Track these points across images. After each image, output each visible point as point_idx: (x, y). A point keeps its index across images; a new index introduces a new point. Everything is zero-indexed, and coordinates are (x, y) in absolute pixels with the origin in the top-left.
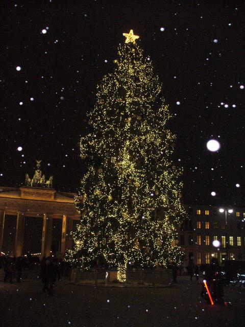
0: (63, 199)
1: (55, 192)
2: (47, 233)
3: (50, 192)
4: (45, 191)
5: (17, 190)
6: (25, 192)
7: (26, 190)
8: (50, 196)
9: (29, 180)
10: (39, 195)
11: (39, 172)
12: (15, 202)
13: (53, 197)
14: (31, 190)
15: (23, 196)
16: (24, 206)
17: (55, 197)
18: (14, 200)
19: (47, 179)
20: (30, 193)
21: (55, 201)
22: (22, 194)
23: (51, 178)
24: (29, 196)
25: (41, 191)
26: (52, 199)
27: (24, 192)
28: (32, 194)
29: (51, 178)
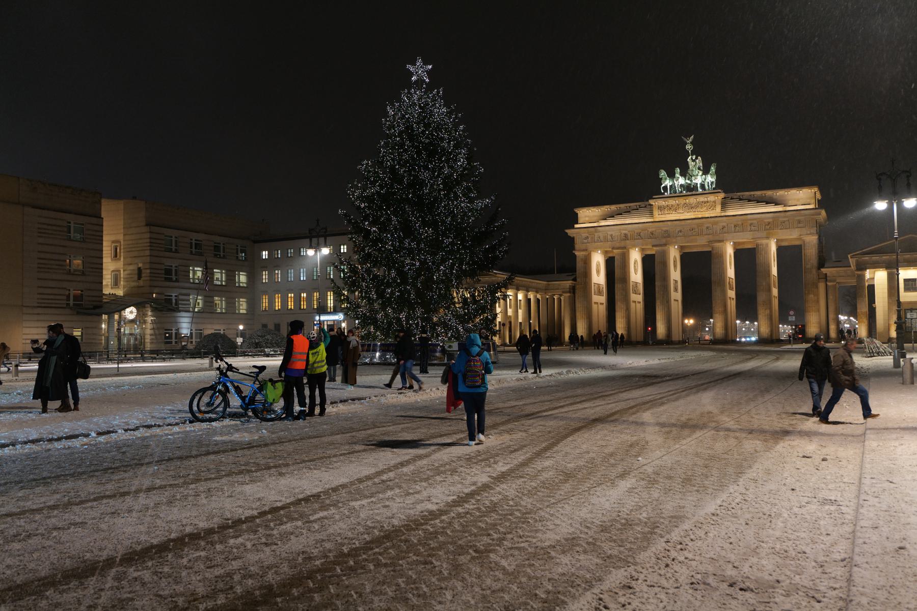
0: (742, 207)
1: (722, 195)
3: (711, 198)
4: (701, 199)
6: (660, 208)
7: (661, 202)
8: (713, 206)
9: (668, 183)
10: (691, 207)
11: (693, 161)
12: (644, 230)
13: (719, 208)
14: (671, 202)
15: (658, 216)
17: (724, 206)
20: (670, 208)
21: (723, 214)
23: (713, 169)
24: (666, 212)
25: (692, 200)
26: (717, 211)
27: (660, 208)
28: (674, 208)
29: (713, 169)
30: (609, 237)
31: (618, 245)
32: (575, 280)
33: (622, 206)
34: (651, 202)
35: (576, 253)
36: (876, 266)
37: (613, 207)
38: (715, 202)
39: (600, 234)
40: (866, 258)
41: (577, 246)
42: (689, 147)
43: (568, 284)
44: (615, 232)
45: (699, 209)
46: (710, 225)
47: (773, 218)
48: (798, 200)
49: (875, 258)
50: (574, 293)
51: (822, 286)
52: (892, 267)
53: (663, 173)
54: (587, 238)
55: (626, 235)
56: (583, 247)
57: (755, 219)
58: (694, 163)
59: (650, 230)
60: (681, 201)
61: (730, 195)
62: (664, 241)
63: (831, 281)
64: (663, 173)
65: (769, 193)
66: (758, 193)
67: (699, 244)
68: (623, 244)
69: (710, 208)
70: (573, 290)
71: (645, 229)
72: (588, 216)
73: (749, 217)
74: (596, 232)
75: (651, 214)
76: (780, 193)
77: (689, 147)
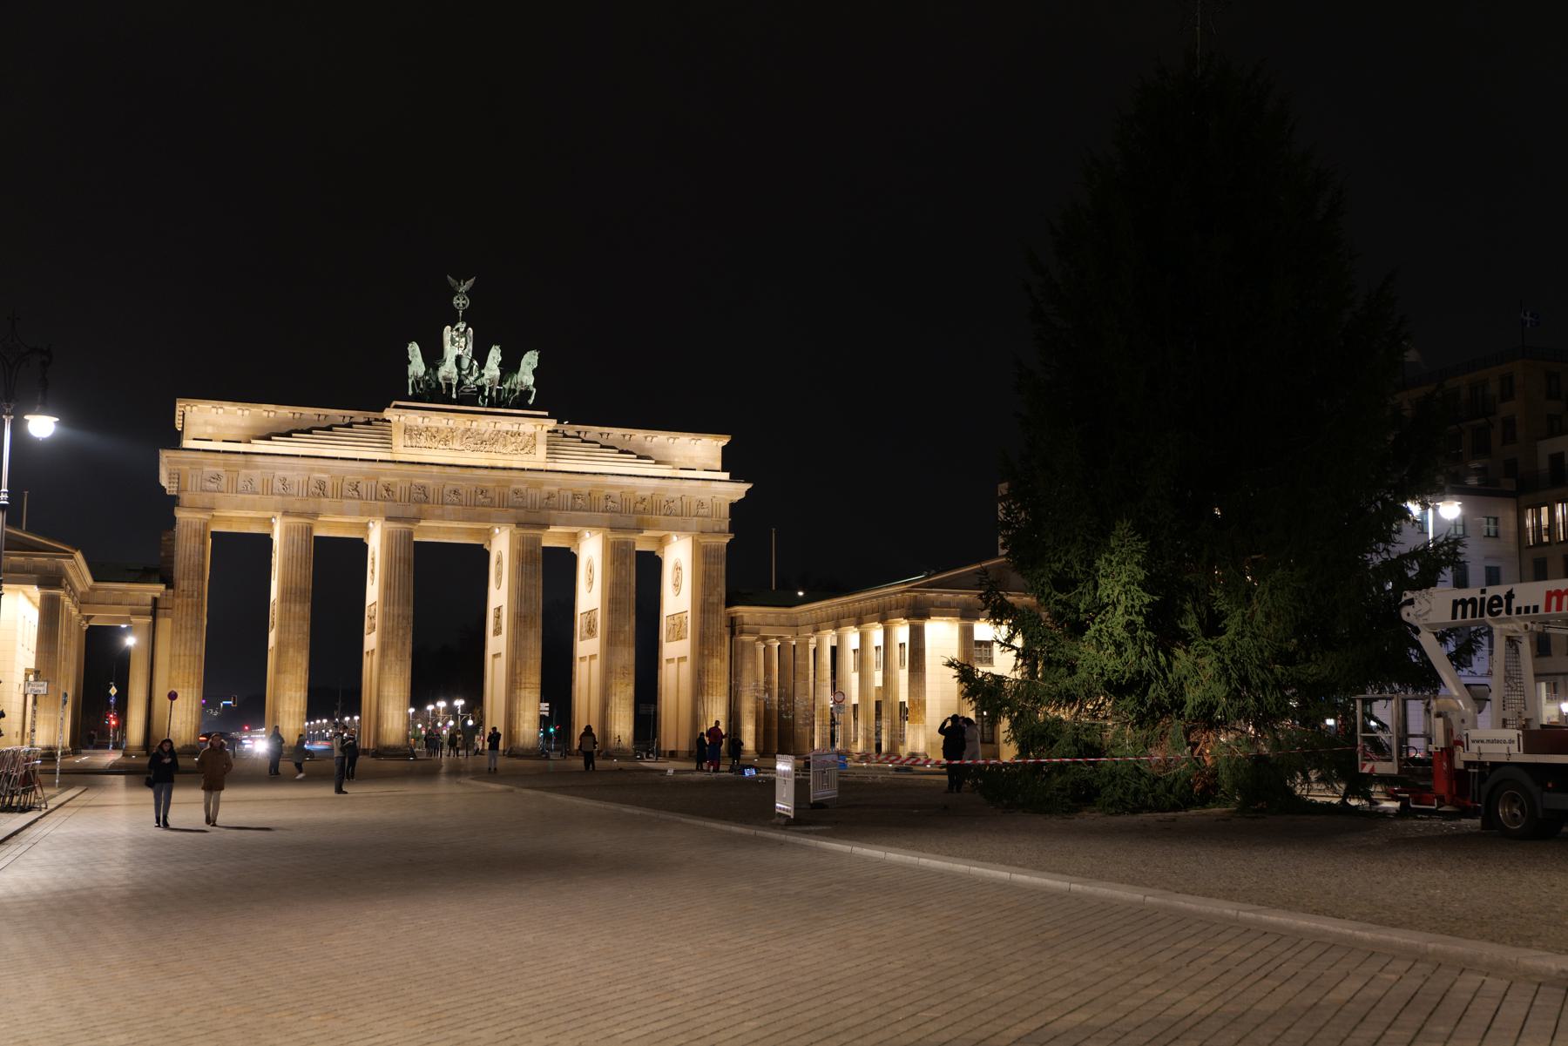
1: (551, 424)
2: (520, 619)
4: (505, 424)
5: (368, 423)
6: (408, 431)
7: (414, 418)
10: (483, 442)
13: (542, 450)
15: (402, 449)
16: (408, 498)
17: (553, 450)
18: (366, 465)
19: (510, 366)
20: (433, 434)
21: (550, 466)
22: (398, 440)
23: (530, 360)
24: (423, 440)
25: (485, 424)
26: (538, 458)
28: (446, 438)
29: (530, 360)
30: (278, 485)
31: (298, 506)
32: (169, 582)
33: (309, 413)
34: (389, 414)
35: (180, 514)
36: (944, 610)
37: (285, 412)
38: (534, 436)
39: (256, 474)
40: (932, 595)
41: (185, 498)
42: (460, 302)
43: (157, 589)
44: (296, 474)
45: (498, 447)
46: (522, 487)
47: (656, 489)
48: (692, 459)
49: (947, 596)
50: (154, 614)
51: (727, 639)
52: (967, 614)
53: (414, 350)
54: (218, 477)
55: (321, 485)
56: (205, 499)
57: (617, 487)
58: (456, 344)
59: (383, 479)
60: (459, 422)
61: (561, 428)
62: (413, 510)
63: (752, 633)
64: (414, 350)
65: (639, 435)
66: (616, 433)
67: (440, 530)
68: (310, 505)
69: (521, 445)
70: (155, 608)
71: (375, 477)
72: (208, 422)
73: (610, 479)
74: (246, 466)
75: (386, 441)
76: (659, 440)
77: (460, 302)
